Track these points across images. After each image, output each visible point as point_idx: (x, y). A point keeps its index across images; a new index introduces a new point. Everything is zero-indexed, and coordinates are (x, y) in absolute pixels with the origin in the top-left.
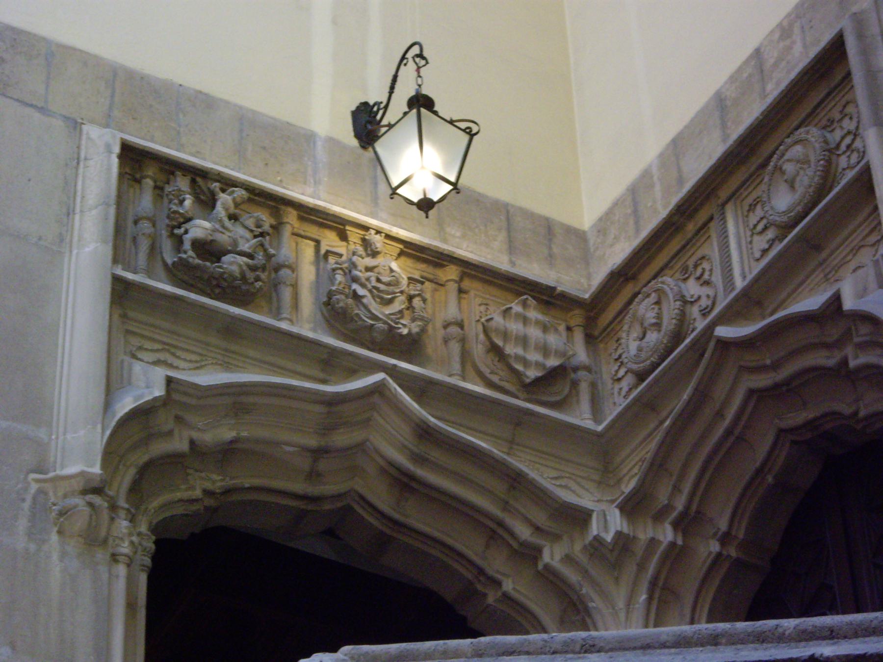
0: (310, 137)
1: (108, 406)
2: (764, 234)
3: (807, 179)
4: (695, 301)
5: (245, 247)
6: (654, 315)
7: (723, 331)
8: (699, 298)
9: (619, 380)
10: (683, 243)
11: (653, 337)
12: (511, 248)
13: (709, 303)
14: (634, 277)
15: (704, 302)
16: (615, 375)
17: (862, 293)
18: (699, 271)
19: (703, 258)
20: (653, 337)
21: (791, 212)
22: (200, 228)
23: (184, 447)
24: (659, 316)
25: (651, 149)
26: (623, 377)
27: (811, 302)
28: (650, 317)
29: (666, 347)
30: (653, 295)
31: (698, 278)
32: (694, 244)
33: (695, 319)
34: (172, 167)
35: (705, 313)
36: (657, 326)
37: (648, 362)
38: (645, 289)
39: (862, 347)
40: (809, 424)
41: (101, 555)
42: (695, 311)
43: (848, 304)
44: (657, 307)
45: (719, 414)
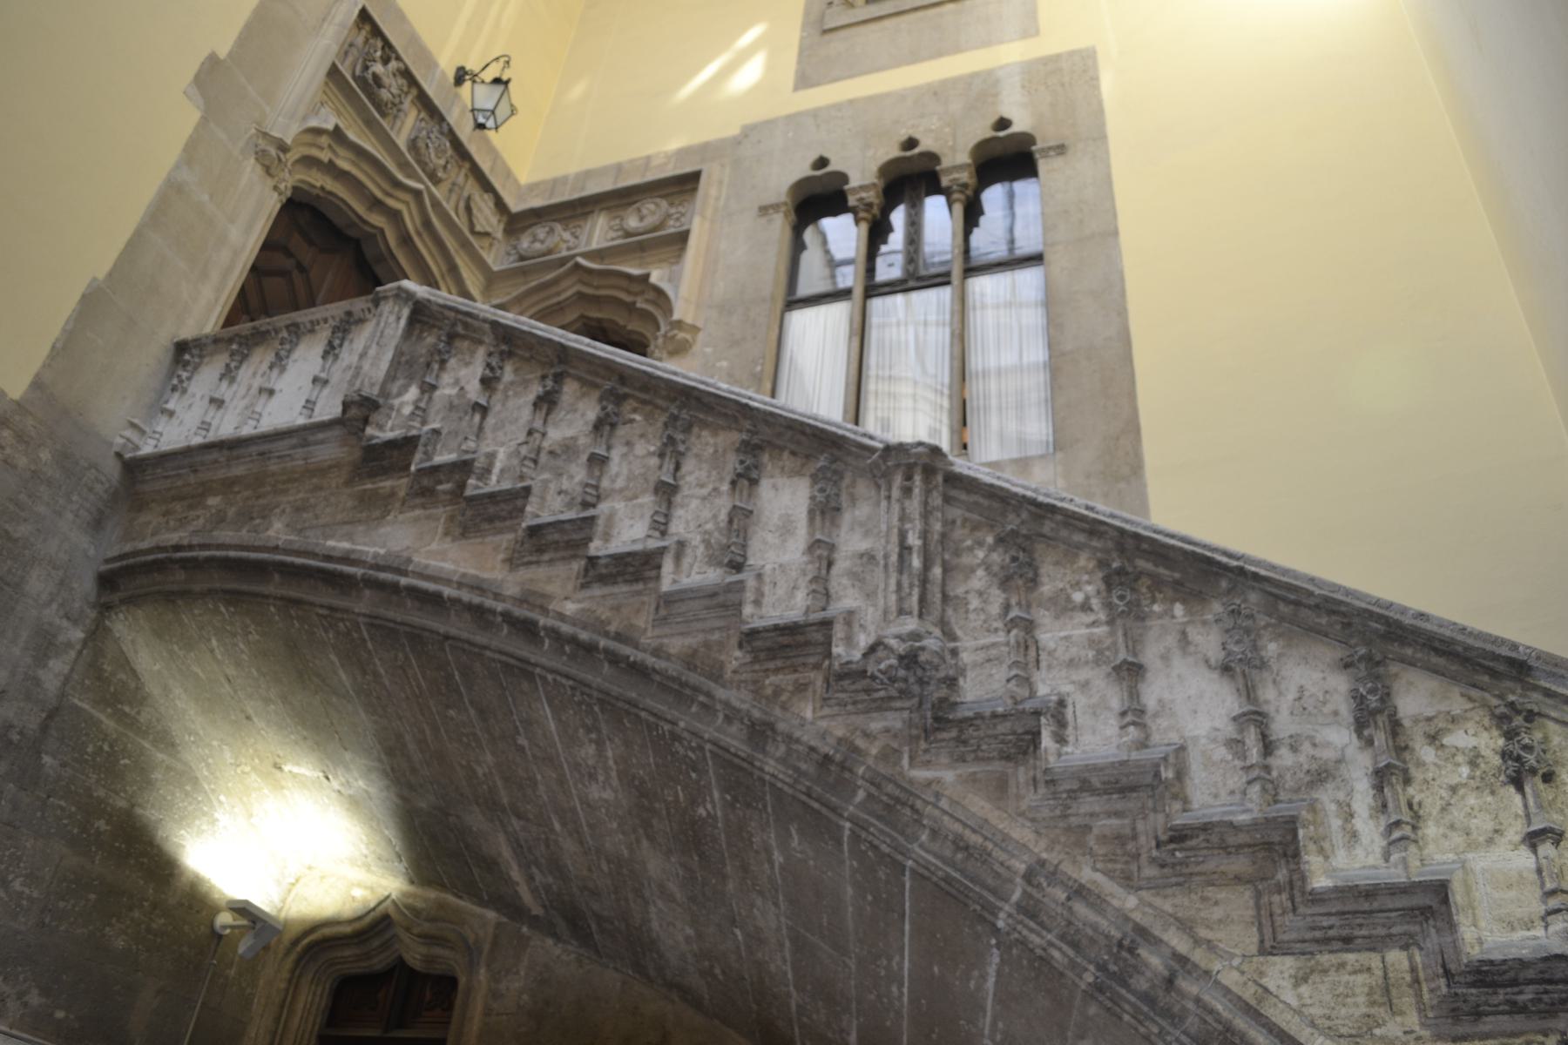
0: (436, 65)
1: (305, 118)
3: (650, 221)
5: (394, 91)
7: (580, 260)
11: (537, 246)
12: (492, 169)
17: (661, 279)
20: (537, 246)
22: (378, 68)
23: (326, 160)
25: (573, 168)
27: (635, 271)
34: (377, 32)
39: (647, 301)
40: (599, 320)
41: (270, 182)
43: (654, 279)
45: (558, 294)
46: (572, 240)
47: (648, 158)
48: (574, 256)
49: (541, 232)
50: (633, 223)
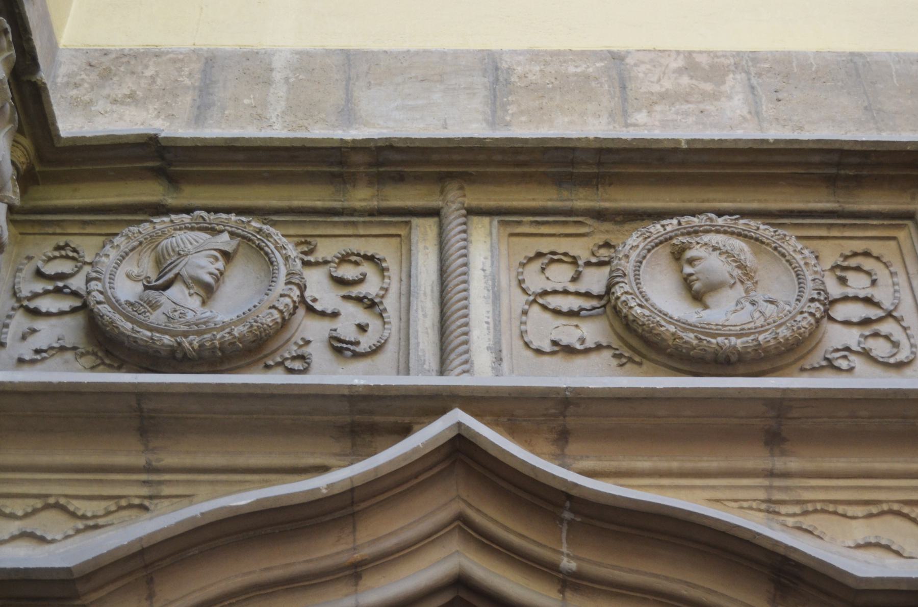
2: (562, 321)
4: (323, 314)
6: (212, 268)
8: (335, 315)
9: (35, 313)
10: (336, 205)
13: (366, 342)
14: (174, 180)
15: (346, 329)
16: (29, 299)
18: (348, 272)
19: (371, 259)
21: (738, 336)
24: (219, 277)
26: (48, 314)
28: (203, 265)
29: (233, 344)
30: (225, 237)
31: (340, 282)
32: (354, 224)
33: (307, 342)
35: (340, 348)
36: (208, 291)
37: (167, 340)
38: (204, 214)
42: (314, 331)
44: (220, 264)
46: (352, 314)
47: (617, 58)
48: (434, 403)
49: (198, 250)
50: (660, 297)
